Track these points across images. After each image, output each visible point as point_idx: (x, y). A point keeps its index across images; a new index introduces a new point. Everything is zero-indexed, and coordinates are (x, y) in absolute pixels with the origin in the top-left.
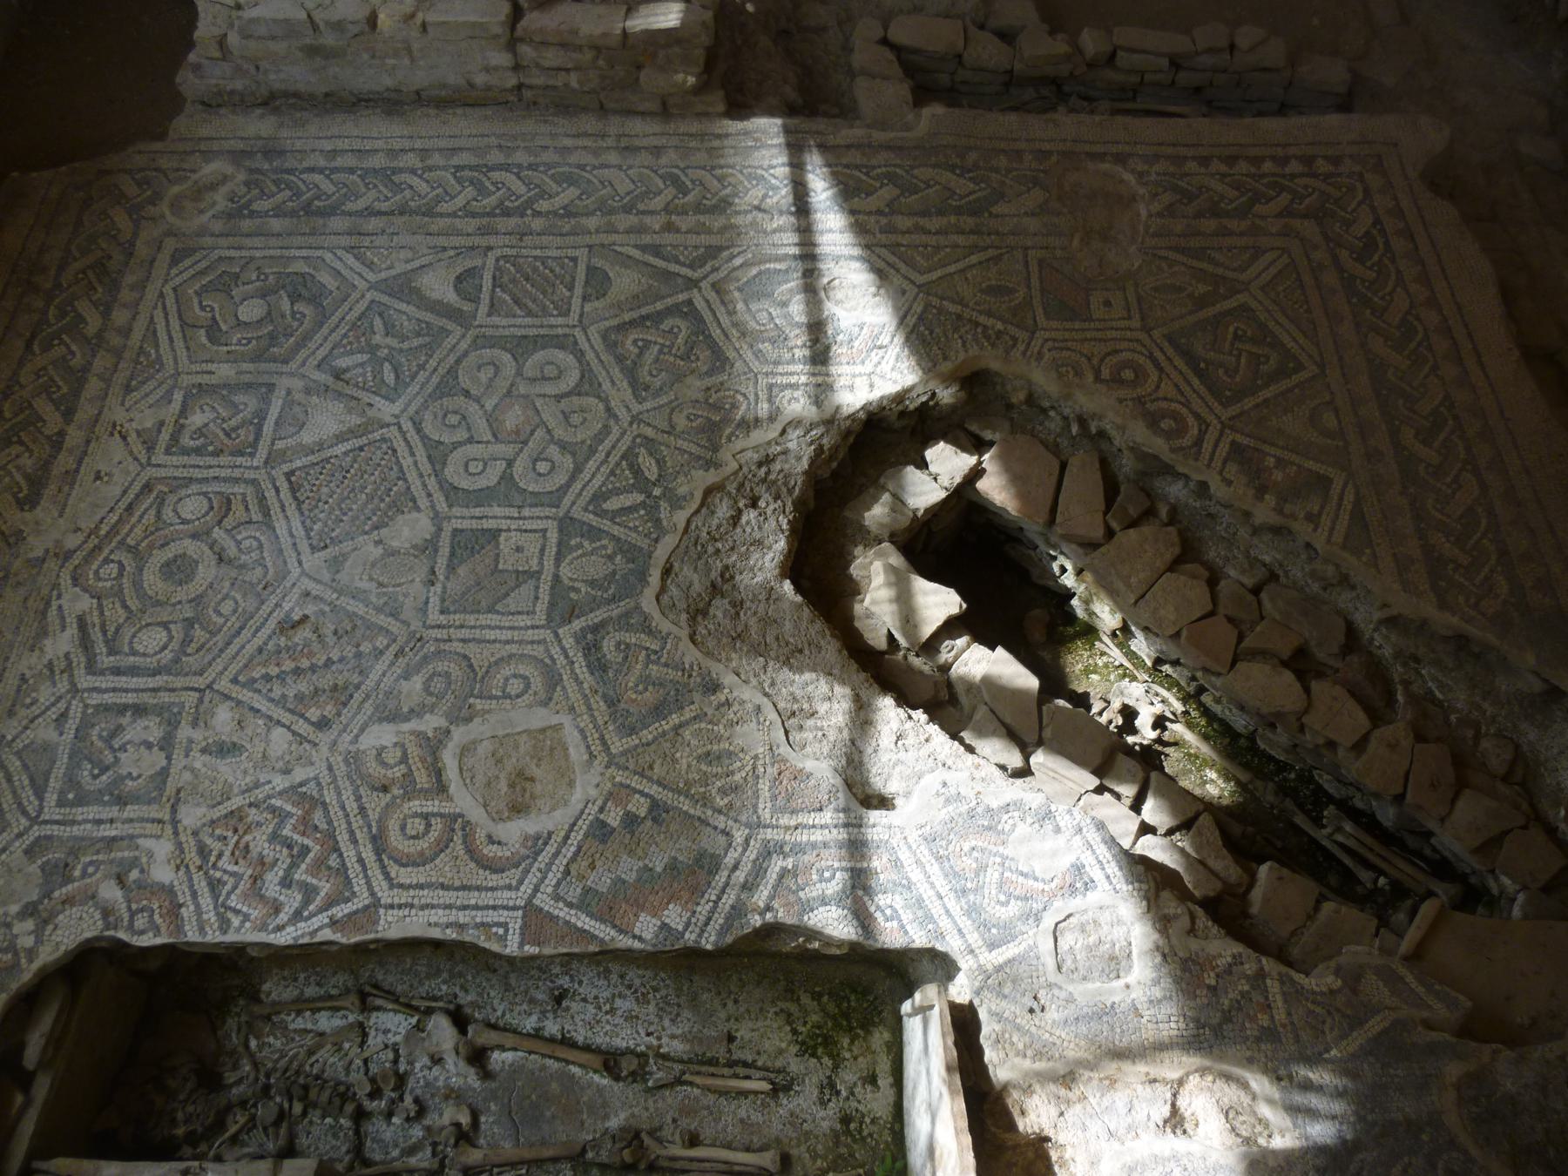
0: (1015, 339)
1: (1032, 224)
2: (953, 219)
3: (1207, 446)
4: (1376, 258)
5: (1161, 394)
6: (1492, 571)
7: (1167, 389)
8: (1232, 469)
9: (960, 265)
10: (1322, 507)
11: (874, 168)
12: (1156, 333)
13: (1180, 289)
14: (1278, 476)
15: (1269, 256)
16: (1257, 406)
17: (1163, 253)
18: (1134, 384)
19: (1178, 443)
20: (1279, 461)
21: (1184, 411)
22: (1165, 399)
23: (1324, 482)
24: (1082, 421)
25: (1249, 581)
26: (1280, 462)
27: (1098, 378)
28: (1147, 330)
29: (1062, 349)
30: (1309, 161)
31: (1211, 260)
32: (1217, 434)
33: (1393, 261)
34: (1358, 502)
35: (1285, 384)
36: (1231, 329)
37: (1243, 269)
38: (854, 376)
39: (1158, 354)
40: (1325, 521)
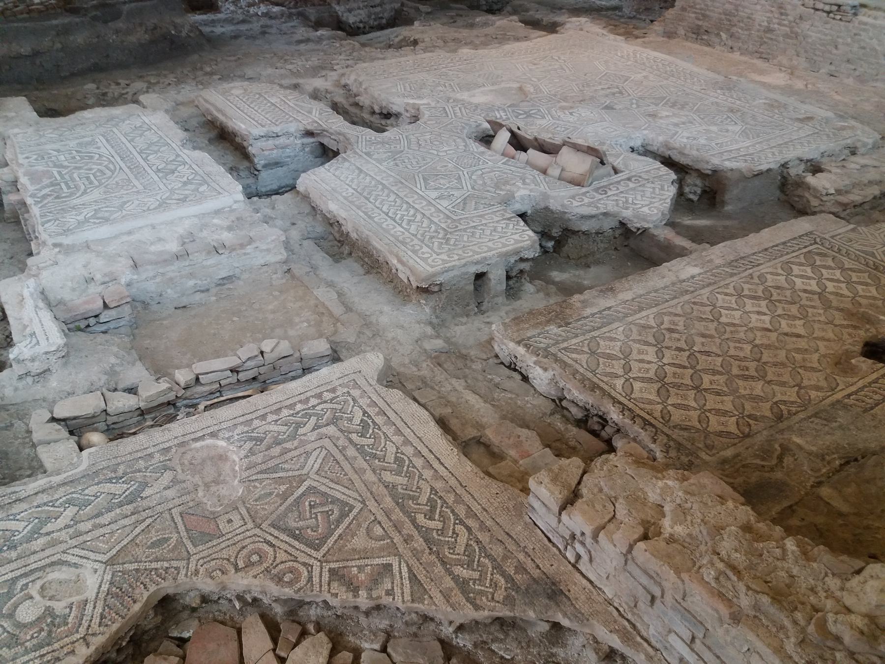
0: (177, 569)
1: (170, 493)
2: (118, 511)
3: (316, 580)
4: (371, 431)
5: (278, 561)
6: (492, 575)
7: (281, 556)
8: (335, 585)
9: (130, 538)
10: (393, 583)
11: (57, 500)
12: (264, 526)
13: (271, 494)
14: (362, 577)
15: (315, 454)
16: (336, 541)
17: (254, 477)
18: (260, 562)
19: (298, 586)
20: (359, 567)
21: (295, 564)
22: (282, 562)
23: (388, 567)
24: (240, 598)
25: (377, 646)
26: (360, 568)
27: (237, 570)
28: (259, 526)
29: (209, 561)
30: (319, 396)
31: (283, 470)
32: (319, 569)
33: (379, 429)
34: (410, 570)
35: (347, 521)
36: (307, 503)
37: (303, 467)
38: (73, 643)
39: (270, 538)
40: (397, 590)
